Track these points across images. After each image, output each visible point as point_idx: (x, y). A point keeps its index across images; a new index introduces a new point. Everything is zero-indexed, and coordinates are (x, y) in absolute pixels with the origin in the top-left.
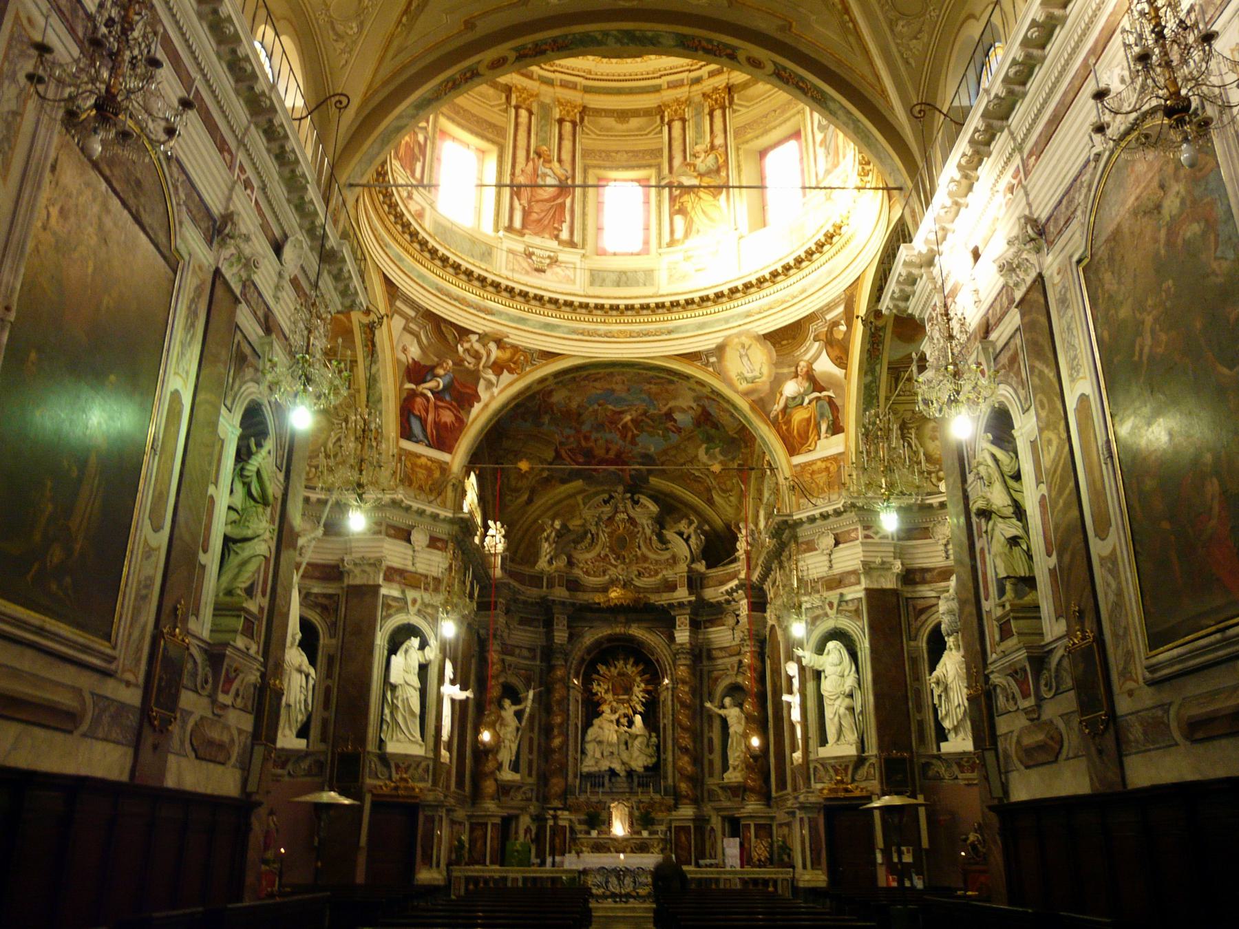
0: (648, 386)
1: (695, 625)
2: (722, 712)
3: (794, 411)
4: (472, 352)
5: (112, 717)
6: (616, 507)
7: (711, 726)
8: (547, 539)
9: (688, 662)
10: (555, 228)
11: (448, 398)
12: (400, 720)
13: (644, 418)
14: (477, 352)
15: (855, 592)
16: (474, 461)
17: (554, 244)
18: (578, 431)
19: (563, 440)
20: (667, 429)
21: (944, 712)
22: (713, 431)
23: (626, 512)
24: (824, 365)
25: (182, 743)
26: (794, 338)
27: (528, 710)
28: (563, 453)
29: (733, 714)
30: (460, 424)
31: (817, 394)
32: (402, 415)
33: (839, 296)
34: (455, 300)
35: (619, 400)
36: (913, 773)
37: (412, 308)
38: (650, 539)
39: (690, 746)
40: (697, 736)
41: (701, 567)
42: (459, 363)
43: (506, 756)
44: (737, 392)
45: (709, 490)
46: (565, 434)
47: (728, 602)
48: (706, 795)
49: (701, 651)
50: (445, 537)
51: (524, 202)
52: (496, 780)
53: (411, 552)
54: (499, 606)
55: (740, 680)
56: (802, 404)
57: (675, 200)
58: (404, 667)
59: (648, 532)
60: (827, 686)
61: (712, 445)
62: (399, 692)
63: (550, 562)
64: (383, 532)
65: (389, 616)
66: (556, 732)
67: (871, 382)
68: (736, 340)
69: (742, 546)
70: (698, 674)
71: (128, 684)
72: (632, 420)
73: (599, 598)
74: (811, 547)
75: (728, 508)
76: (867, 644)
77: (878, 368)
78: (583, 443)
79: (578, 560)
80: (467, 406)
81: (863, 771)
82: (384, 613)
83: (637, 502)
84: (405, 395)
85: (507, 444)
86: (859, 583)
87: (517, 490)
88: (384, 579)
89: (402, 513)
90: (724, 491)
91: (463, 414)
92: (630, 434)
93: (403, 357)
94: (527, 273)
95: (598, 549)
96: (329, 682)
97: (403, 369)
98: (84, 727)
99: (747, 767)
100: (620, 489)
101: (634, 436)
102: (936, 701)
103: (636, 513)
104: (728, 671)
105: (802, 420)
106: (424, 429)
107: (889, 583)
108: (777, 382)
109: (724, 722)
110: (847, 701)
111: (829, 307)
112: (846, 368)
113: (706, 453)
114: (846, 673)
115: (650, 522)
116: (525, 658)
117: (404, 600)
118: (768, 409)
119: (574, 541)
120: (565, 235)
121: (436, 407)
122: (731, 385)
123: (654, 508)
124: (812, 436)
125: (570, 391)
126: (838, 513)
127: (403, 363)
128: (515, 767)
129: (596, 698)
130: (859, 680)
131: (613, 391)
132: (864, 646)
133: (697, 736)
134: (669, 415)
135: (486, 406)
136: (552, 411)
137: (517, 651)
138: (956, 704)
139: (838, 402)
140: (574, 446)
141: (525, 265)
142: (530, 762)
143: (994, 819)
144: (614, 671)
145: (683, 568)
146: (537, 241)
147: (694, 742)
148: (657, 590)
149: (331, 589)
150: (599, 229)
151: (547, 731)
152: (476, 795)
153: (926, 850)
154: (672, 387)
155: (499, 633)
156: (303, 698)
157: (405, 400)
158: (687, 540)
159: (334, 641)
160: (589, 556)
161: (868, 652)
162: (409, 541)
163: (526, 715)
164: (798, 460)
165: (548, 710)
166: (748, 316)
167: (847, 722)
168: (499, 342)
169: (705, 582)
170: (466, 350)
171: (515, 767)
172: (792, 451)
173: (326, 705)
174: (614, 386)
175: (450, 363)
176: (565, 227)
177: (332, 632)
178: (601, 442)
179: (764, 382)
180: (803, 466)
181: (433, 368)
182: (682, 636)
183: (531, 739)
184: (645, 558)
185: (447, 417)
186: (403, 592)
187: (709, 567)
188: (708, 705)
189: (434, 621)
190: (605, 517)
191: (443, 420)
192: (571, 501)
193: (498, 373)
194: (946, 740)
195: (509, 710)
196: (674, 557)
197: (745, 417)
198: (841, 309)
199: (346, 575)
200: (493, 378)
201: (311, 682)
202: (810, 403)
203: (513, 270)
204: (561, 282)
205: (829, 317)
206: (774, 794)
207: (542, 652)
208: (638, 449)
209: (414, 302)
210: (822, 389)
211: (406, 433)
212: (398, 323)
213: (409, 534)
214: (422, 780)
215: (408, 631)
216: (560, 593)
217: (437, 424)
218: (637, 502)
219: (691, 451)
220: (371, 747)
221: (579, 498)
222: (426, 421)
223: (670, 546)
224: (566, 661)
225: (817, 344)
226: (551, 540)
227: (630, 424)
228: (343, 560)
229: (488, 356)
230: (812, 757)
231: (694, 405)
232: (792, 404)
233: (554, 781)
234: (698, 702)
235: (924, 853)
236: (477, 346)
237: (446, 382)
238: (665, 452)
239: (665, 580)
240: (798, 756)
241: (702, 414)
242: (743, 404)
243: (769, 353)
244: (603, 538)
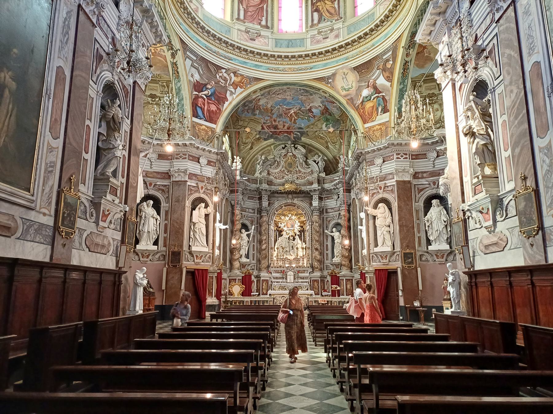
0: (301, 97)
1: (321, 199)
2: (332, 234)
3: (366, 103)
4: (223, 77)
5: (35, 230)
6: (288, 150)
7: (327, 240)
8: (259, 164)
9: (318, 214)
10: (259, 19)
11: (213, 99)
12: (197, 237)
13: (299, 111)
14: (225, 77)
15: (391, 182)
16: (226, 130)
17: (259, 27)
18: (271, 118)
19: (265, 122)
20: (309, 116)
21: (430, 233)
22: (329, 117)
23: (292, 152)
24: (381, 81)
25: (80, 244)
27: (252, 234)
28: (265, 127)
29: (336, 235)
30: (219, 112)
32: (193, 106)
33: (390, 46)
34: (214, 52)
35: (289, 103)
36: (415, 257)
37: (195, 56)
38: (302, 163)
39: (319, 248)
40: (322, 244)
41: (323, 175)
42: (217, 83)
43: (243, 252)
44: (341, 95)
45: (327, 142)
46: (266, 119)
47: (334, 189)
48: (325, 267)
49: (323, 210)
50: (214, 161)
51: (245, 6)
52: (240, 262)
53: (200, 167)
54: (239, 191)
55: (339, 221)
56: (370, 100)
57: (314, 5)
58: (199, 214)
59: (301, 161)
60: (378, 222)
61: (328, 123)
62: (197, 226)
63: (260, 173)
64: (187, 158)
65: (191, 194)
66: (264, 242)
67: (403, 88)
68: (341, 71)
69: (341, 166)
70: (322, 219)
71: (44, 214)
72: (294, 112)
73: (281, 188)
74: (372, 163)
75: (335, 150)
76: (396, 204)
77: (406, 81)
78: (273, 122)
79: (272, 172)
80: (222, 103)
81: (394, 258)
82: (189, 193)
83: (296, 148)
84: (194, 97)
85: (241, 123)
86: (394, 178)
87: (245, 144)
88: (189, 179)
89: (195, 150)
90: (333, 143)
91: (220, 106)
92: (293, 119)
93: (192, 79)
94: (247, 41)
95: (280, 167)
96: (166, 222)
97: (192, 85)
98: (18, 234)
99: (342, 256)
100: (289, 142)
101: (295, 120)
102: (427, 228)
103: (296, 152)
104: (333, 217)
105: (369, 108)
106: (203, 113)
107: (407, 178)
108: (359, 90)
109: (333, 238)
110: (388, 229)
111: (385, 53)
112: (391, 82)
113: (326, 127)
114: (387, 217)
115: (302, 156)
116: (250, 213)
117: (198, 187)
118: (355, 103)
119: (270, 165)
120: (263, 23)
121: (208, 103)
122: (338, 93)
123: (304, 151)
124: (374, 114)
125: (267, 99)
126: (385, 148)
128: (247, 256)
129: (280, 229)
130: (392, 219)
131: (286, 99)
132: (395, 205)
133: (322, 244)
134: (310, 110)
135: (231, 103)
136: (260, 108)
137: (247, 210)
138: (436, 229)
139: (387, 98)
140: (269, 124)
141: (246, 37)
142: (254, 254)
143: (466, 278)
144: (287, 218)
145: (315, 175)
146: (251, 25)
147: (320, 246)
148: (304, 185)
149: (166, 182)
150: (280, 20)
151: (260, 242)
152: (231, 268)
153: (421, 290)
154: (312, 97)
155: (239, 202)
156: (155, 229)
157: (194, 99)
158: (317, 164)
159: (167, 205)
160: (276, 171)
161: (397, 208)
162: (199, 162)
163: (251, 236)
164: (367, 125)
165: (260, 233)
166: (346, 59)
167: (387, 237)
168: (235, 73)
169: (325, 181)
170: (220, 77)
171: (247, 256)
172: (365, 122)
173: (165, 232)
174: (287, 97)
175: (213, 82)
176: (264, 18)
177: (167, 201)
178: (281, 122)
179: (353, 90)
180: (370, 128)
181: (206, 85)
182: (315, 203)
183: (254, 245)
184: (300, 172)
185: (213, 108)
186: (197, 184)
187: (326, 175)
188: (326, 231)
189: (211, 197)
190: (283, 154)
191: (211, 109)
192: (269, 148)
194: (431, 245)
195: (244, 234)
196: (312, 171)
197: (345, 107)
198: (390, 53)
199: (172, 177)
200: (233, 90)
201: (158, 222)
202: (374, 99)
203: (240, 39)
204: (262, 45)
205: (384, 58)
206: (353, 267)
207: (258, 210)
208: (297, 126)
209: (195, 52)
210: (380, 92)
211: (195, 115)
212: (188, 62)
213: (199, 159)
214: (207, 262)
215: (200, 200)
216: (265, 186)
217: (208, 111)
218: (296, 148)
219: (319, 125)
220: (185, 248)
221: (272, 147)
222: (204, 109)
223: (310, 166)
224: (268, 215)
225: (378, 71)
226: (260, 164)
227: (293, 114)
228: (170, 170)
229: (231, 80)
230: (371, 252)
231: (321, 105)
232: (366, 100)
233: (263, 262)
234: (322, 230)
235: (420, 292)
236: (225, 75)
238: (308, 127)
239: (308, 180)
240: (365, 252)
241: (324, 109)
242: (343, 101)
243: (356, 76)
244: (282, 163)
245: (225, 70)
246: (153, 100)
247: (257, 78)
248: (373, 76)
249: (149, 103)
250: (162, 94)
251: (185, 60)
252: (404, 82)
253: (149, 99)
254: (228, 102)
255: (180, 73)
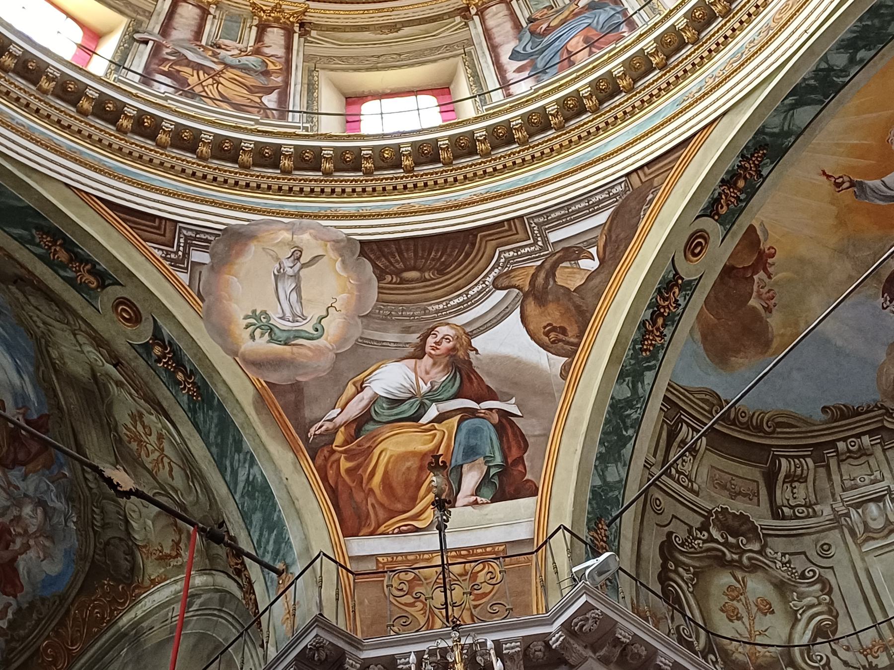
26: (441, 272)
31: (471, 404)
68: (286, 235)
77: (649, 376)
179: (319, 351)
198: (602, 218)
210: (492, 395)
225: (500, 294)
248: (459, 313)
252: (638, 377)
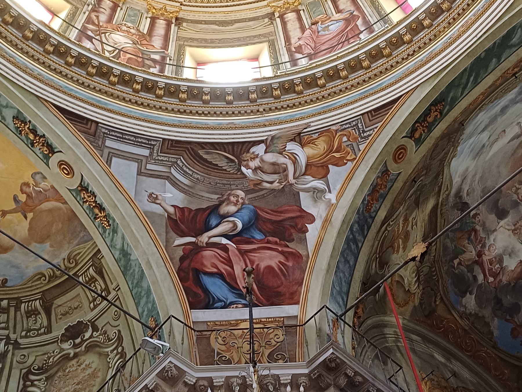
4: (266, 167)
14: (274, 164)
37: (140, 145)
80: (295, 235)
93: (156, 208)
127: (160, 215)
135: (327, 221)
170: (255, 170)
175: (241, 194)
193: (324, 176)
200: (319, 184)
229: (295, 162)
236: (270, 158)
237: (246, 218)
245: (262, 146)
246: (78, 341)
247: (375, 110)
249: (67, 358)
250: (95, 307)
251: (109, 162)
253: (66, 346)
254: (318, 223)
255: (105, 205)
